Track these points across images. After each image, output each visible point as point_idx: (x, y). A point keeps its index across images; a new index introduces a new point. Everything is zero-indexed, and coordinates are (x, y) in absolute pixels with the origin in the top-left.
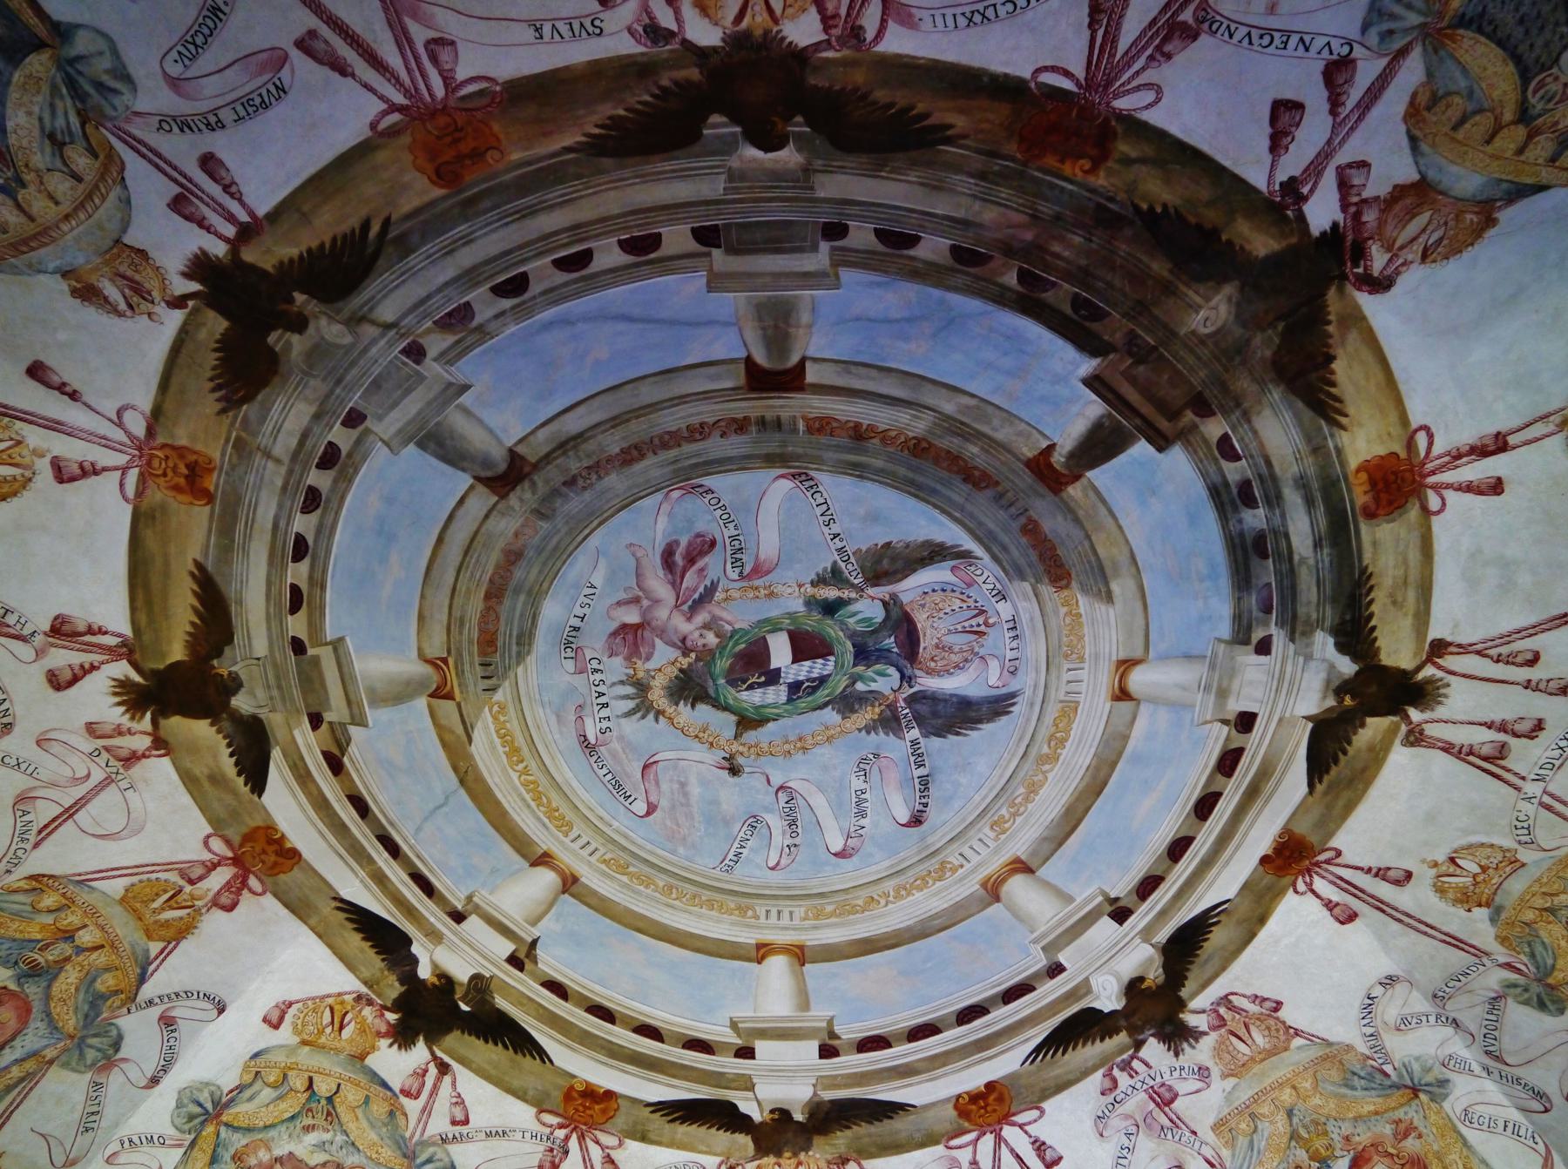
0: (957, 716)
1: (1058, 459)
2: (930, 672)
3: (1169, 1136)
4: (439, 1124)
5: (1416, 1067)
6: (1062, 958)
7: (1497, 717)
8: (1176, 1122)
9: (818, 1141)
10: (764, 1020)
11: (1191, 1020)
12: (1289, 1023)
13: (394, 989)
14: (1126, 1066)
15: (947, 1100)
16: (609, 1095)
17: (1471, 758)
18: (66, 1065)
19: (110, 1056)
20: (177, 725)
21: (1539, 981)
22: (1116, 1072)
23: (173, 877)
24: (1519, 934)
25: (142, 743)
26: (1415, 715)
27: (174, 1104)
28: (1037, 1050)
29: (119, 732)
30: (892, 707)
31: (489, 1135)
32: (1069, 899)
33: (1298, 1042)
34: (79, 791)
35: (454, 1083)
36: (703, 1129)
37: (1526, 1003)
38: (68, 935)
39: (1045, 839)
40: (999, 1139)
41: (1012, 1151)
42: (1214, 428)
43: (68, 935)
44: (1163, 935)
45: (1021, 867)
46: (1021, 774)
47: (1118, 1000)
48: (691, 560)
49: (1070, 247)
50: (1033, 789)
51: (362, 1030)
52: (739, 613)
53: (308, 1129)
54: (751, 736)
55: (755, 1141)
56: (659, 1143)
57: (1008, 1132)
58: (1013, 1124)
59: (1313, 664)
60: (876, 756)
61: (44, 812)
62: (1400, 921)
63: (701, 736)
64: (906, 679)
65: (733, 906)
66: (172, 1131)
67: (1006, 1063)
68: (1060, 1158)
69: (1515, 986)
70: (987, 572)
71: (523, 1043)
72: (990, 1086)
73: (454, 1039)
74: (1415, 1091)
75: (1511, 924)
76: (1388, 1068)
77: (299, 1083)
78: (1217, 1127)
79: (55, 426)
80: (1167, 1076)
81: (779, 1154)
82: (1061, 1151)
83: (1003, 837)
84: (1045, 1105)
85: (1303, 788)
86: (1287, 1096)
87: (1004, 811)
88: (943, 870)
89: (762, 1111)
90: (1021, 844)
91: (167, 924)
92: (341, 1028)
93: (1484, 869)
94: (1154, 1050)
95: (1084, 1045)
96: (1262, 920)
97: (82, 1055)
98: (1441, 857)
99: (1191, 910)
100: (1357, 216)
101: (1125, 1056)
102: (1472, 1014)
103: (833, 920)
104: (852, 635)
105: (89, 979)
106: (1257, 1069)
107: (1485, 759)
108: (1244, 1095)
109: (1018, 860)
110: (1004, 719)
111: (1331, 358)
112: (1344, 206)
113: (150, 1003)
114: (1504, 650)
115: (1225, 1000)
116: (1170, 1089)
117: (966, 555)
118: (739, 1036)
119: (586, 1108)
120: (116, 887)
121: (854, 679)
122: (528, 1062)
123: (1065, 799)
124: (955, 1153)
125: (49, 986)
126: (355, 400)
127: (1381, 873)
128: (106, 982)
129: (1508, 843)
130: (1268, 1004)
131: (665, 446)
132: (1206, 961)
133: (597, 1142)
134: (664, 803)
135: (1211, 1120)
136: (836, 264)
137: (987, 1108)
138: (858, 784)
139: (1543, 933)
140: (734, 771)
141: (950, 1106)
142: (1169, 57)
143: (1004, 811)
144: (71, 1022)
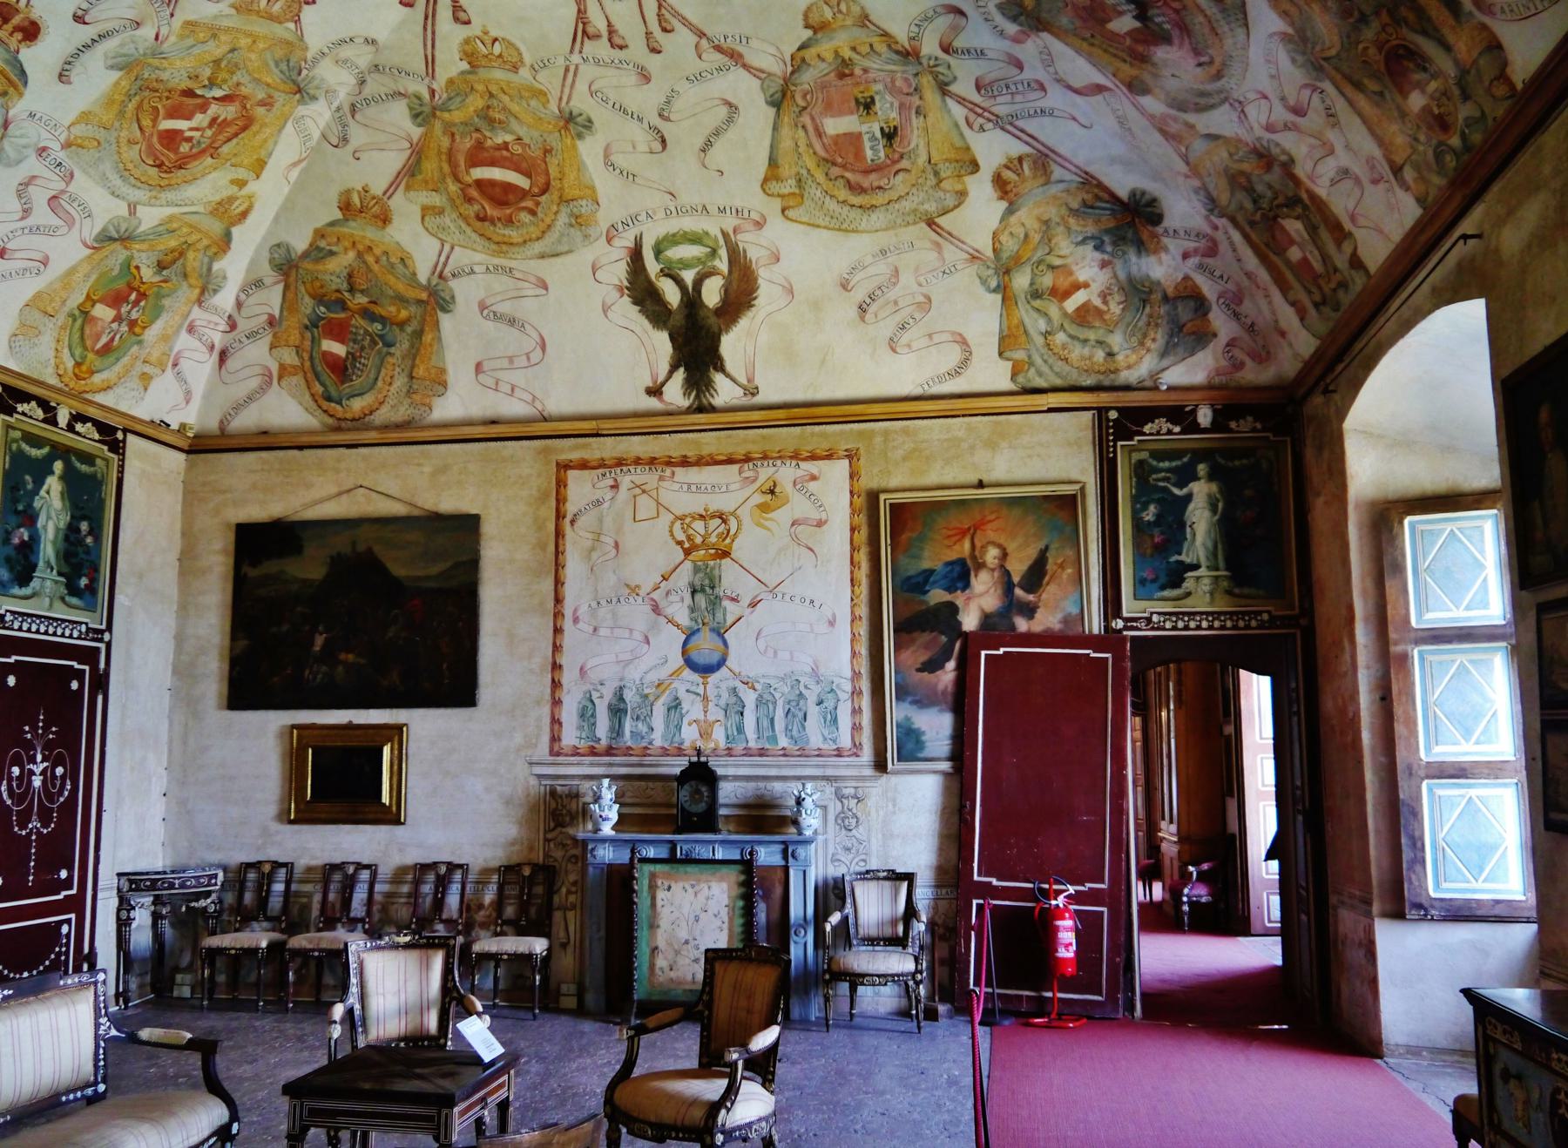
5: (316, 82)
7: (618, 25)
21: (434, 108)
24: (459, 88)
33: (292, 26)
37: (411, 109)
62: (425, 29)
69: (419, 98)
74: (299, 91)
75: (466, 82)
76: (304, 72)
78: (188, 23)
86: (244, 42)
93: (500, 56)
98: (494, 33)
102: (374, 86)
107: (584, 32)
108: (226, 23)
114: (668, 16)
129: (528, 59)
135: (192, 18)
139: (471, 98)
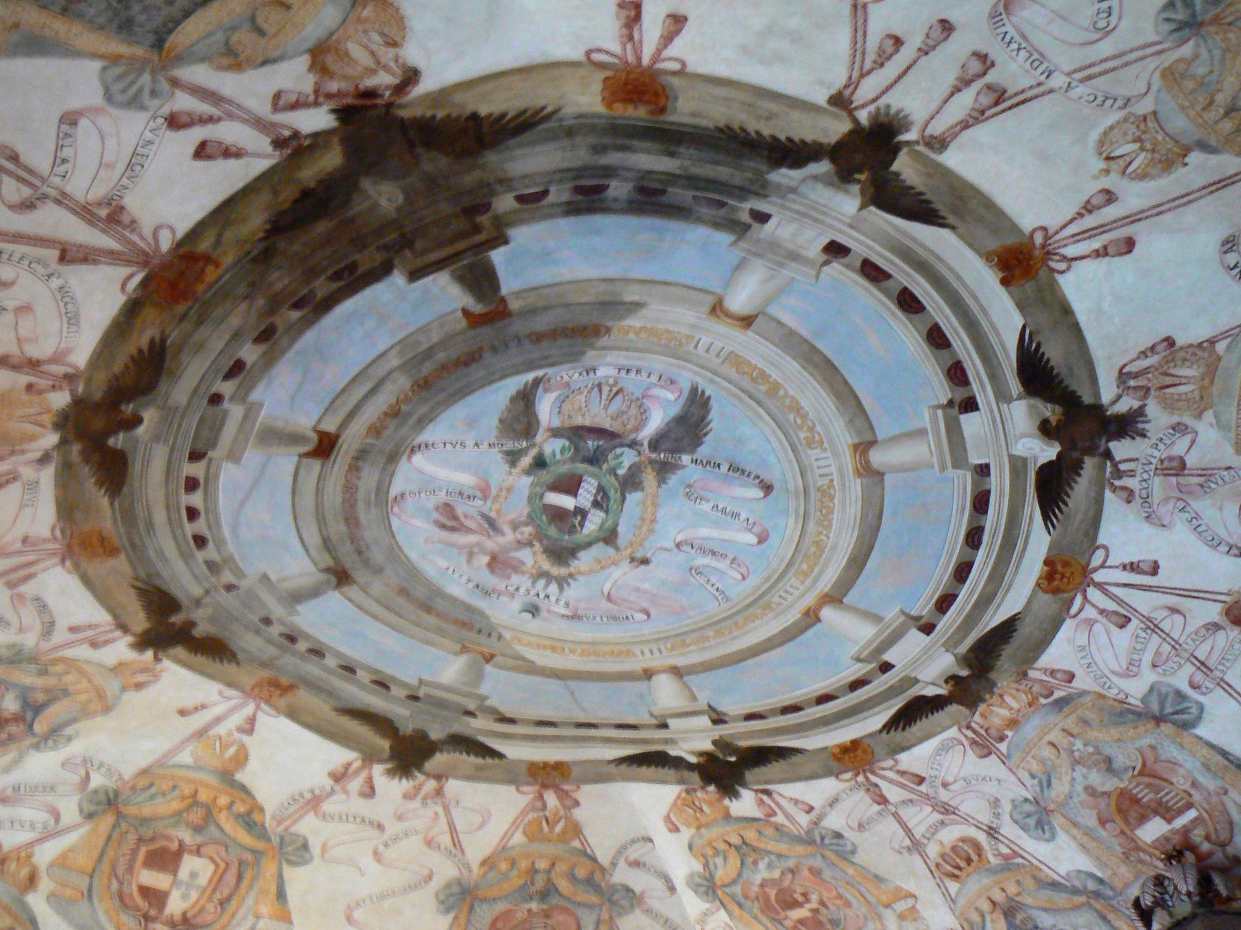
0: (690, 426)
1: (477, 308)
2: (637, 429)
3: (1213, 486)
4: (804, 820)
6: (975, 459)
8: (1207, 474)
9: (992, 675)
10: (869, 643)
11: (1123, 406)
12: (1196, 342)
13: (695, 777)
14: (1119, 474)
15: (1034, 592)
16: (855, 744)
17: (988, 113)
18: (620, 915)
19: (632, 898)
20: (429, 765)
22: (1117, 483)
23: (531, 816)
25: (431, 784)
26: (910, 136)
27: (692, 893)
28: (1046, 517)
29: (418, 789)
30: (651, 462)
31: (831, 806)
32: (922, 432)
33: (1221, 347)
34: (443, 821)
35: (780, 795)
36: (924, 720)
38: (533, 871)
39: (851, 421)
40: (1100, 586)
41: (1117, 585)
42: (505, 203)
43: (533, 871)
44: (1015, 386)
45: (863, 447)
46: (774, 410)
47: (1052, 446)
48: (456, 518)
49: (279, 279)
50: (797, 408)
51: (710, 804)
52: (518, 507)
53: (755, 863)
54: (622, 541)
55: (961, 703)
56: (914, 745)
57: (1098, 577)
58: (1096, 570)
59: (803, 189)
60: (689, 486)
61: (446, 840)
63: (602, 566)
64: (633, 444)
65: (759, 611)
66: (707, 905)
67: (1038, 543)
68: (1156, 562)
70: (566, 373)
71: (782, 753)
72: (1047, 562)
73: (749, 775)
77: (723, 846)
79: (218, 720)
80: (1157, 454)
81: (983, 700)
82: (1153, 557)
83: (826, 444)
84: (1101, 540)
85: (945, 232)
87: (802, 435)
88: (826, 493)
89: (941, 687)
90: (843, 436)
91: (564, 832)
92: (701, 810)
94: (1121, 449)
95: (1072, 488)
96: (1067, 310)
97: (622, 907)
99: (1008, 357)
100: (329, 96)
101: (1109, 469)
103: (817, 570)
104: (573, 460)
105: (572, 877)
106: (1215, 391)
107: (997, 103)
109: (856, 447)
110: (712, 402)
111: (474, 116)
112: (316, 104)
113: (614, 865)
114: (870, 58)
115: (1123, 376)
116: (1171, 459)
117: (537, 382)
118: (869, 662)
119: (853, 757)
120: (518, 838)
121: (613, 472)
122: (796, 759)
123: (822, 392)
124: (1083, 615)
125: (560, 895)
126: (255, 618)
127: (1088, 208)
128: (581, 873)
130: (1160, 348)
131: (353, 506)
132: (1070, 369)
133: (884, 769)
134: (645, 605)
136: (243, 400)
137: (1065, 576)
138: (706, 507)
140: (645, 561)
141: (1040, 594)
142: (133, 222)
143: (802, 435)
144: (594, 899)
